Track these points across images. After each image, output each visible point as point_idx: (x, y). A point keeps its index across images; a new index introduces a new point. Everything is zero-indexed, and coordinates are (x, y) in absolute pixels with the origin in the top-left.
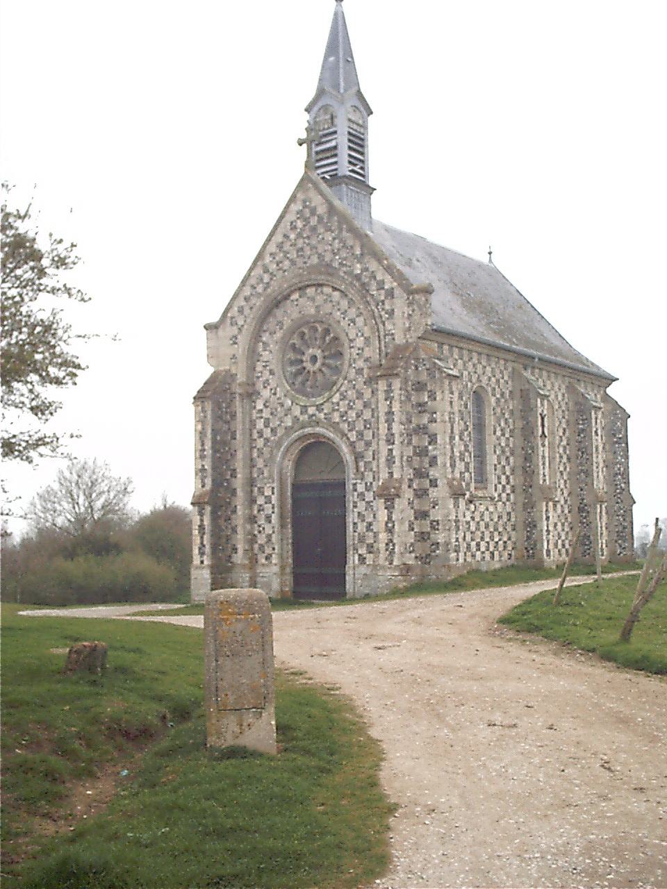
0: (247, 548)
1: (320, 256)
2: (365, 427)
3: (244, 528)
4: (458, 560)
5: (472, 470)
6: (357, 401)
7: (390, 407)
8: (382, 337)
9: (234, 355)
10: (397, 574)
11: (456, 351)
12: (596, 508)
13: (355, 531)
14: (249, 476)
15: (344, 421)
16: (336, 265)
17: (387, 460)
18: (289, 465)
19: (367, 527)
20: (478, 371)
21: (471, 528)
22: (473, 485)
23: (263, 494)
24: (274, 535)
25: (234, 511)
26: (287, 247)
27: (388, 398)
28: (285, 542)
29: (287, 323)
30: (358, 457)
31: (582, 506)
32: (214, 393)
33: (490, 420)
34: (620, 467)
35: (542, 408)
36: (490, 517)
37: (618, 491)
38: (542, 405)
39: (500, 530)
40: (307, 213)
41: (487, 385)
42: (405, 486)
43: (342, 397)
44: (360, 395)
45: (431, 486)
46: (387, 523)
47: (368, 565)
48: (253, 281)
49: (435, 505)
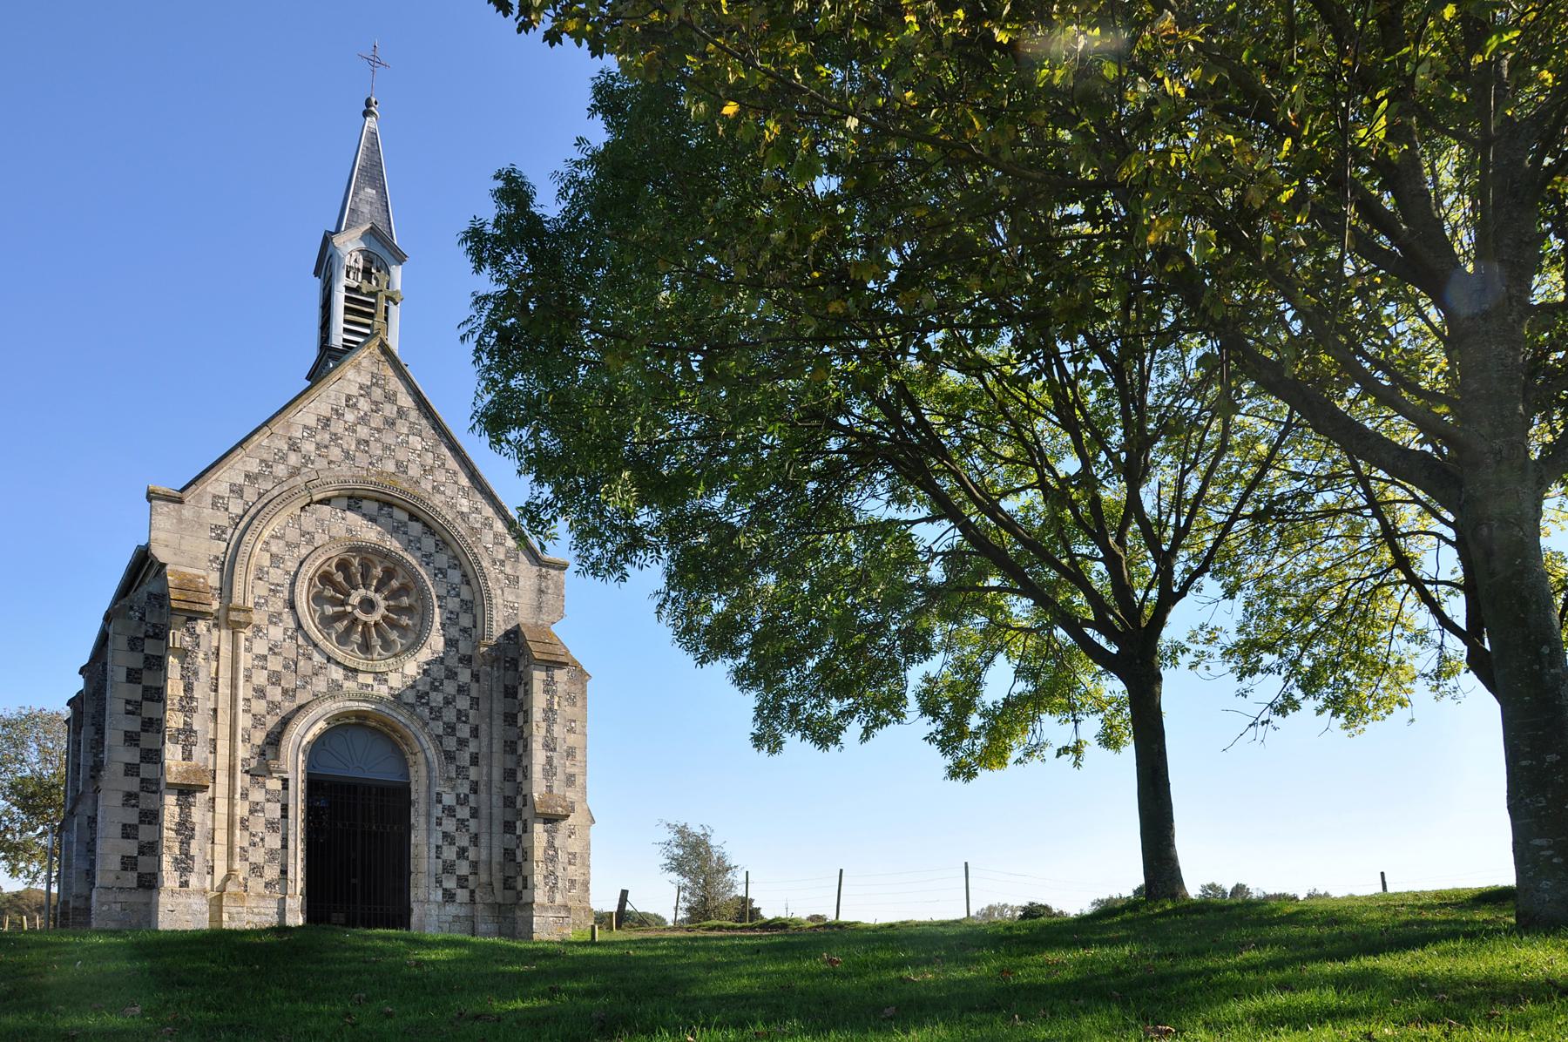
2: (458, 719)
6: (446, 682)
19: (458, 853)
40: (377, 393)
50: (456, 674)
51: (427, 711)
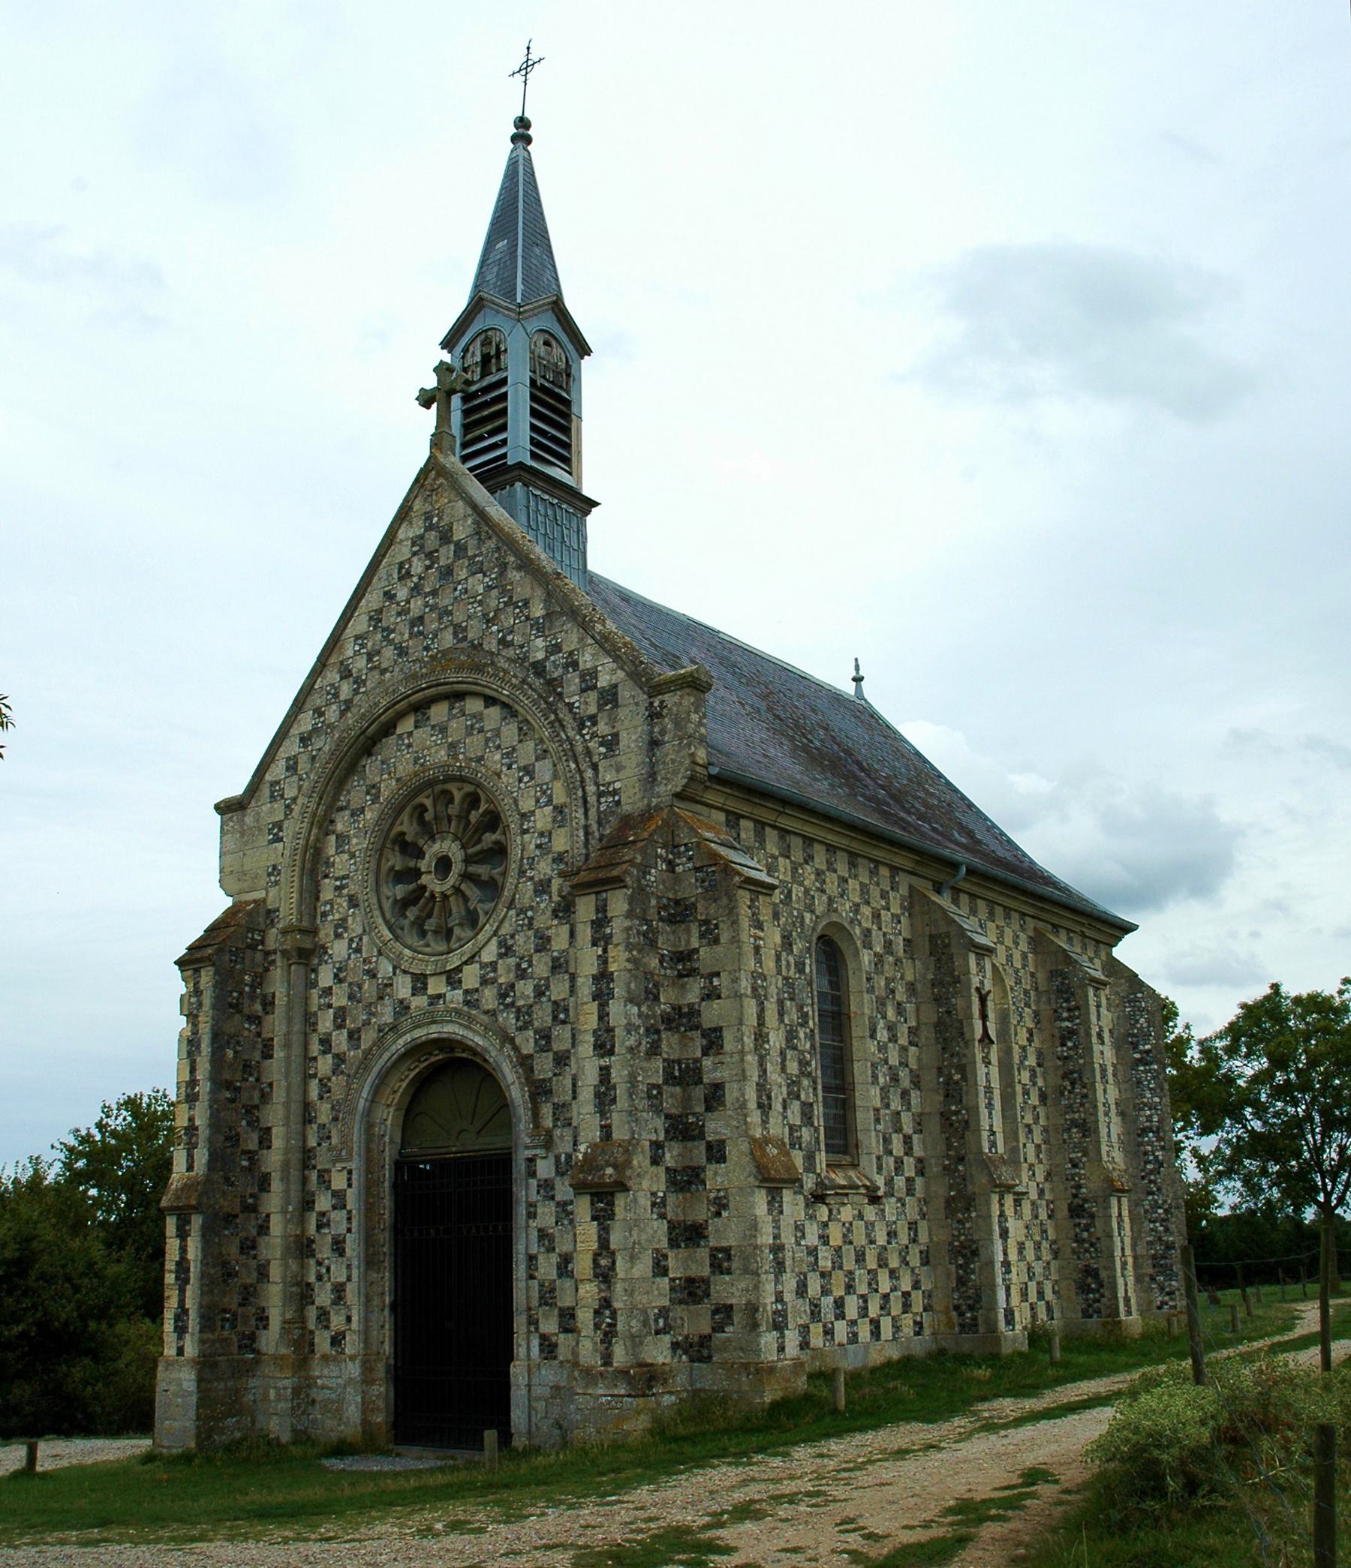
0: (288, 1316)
1: (458, 630)
2: (555, 1018)
3: (286, 1267)
4: (781, 1349)
5: (819, 1121)
6: (536, 957)
7: (603, 960)
8: (592, 799)
9: (274, 867)
10: (622, 1392)
11: (771, 835)
12: (1108, 1207)
14: (301, 1144)
15: (507, 1006)
16: (491, 645)
17: (598, 1095)
18: (388, 1118)
19: (559, 1268)
20: (827, 887)
21: (821, 1263)
22: (821, 1158)
23: (328, 1188)
24: (349, 1287)
25: (264, 1229)
26: (390, 618)
27: (601, 939)
28: (376, 1302)
29: (388, 788)
30: (539, 1091)
31: (1076, 1201)
32: (220, 951)
33: (861, 1005)
34: (1151, 1116)
35: (978, 975)
36: (868, 1235)
37: (1149, 1167)
38: (981, 969)
39: (894, 1262)
41: (852, 922)
42: (641, 1160)
43: (503, 950)
44: (543, 943)
45: (709, 1160)
46: (596, 1256)
47: (562, 1362)
48: (317, 700)
49: (720, 1205)
50: (549, 939)
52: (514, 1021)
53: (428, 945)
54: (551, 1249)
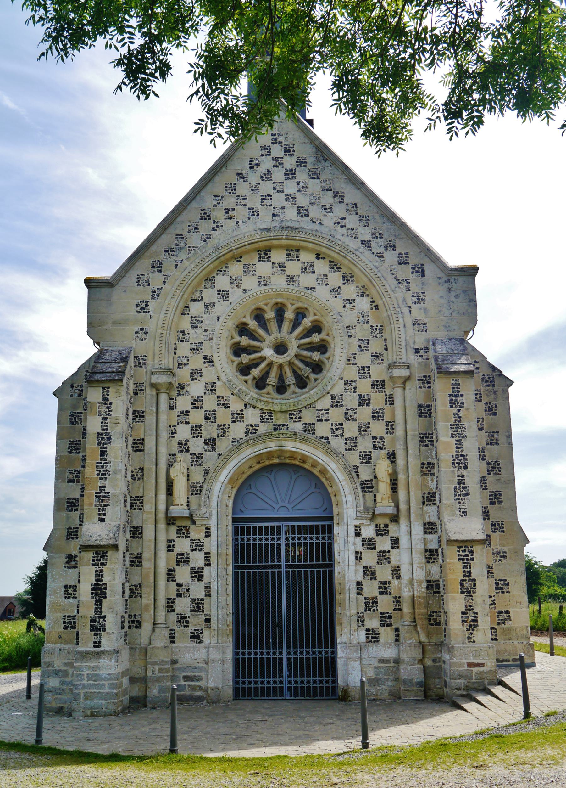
13: (358, 594)
40: (277, 151)
51: (342, 441)
52: (343, 444)
53: (268, 393)
54: (373, 578)
